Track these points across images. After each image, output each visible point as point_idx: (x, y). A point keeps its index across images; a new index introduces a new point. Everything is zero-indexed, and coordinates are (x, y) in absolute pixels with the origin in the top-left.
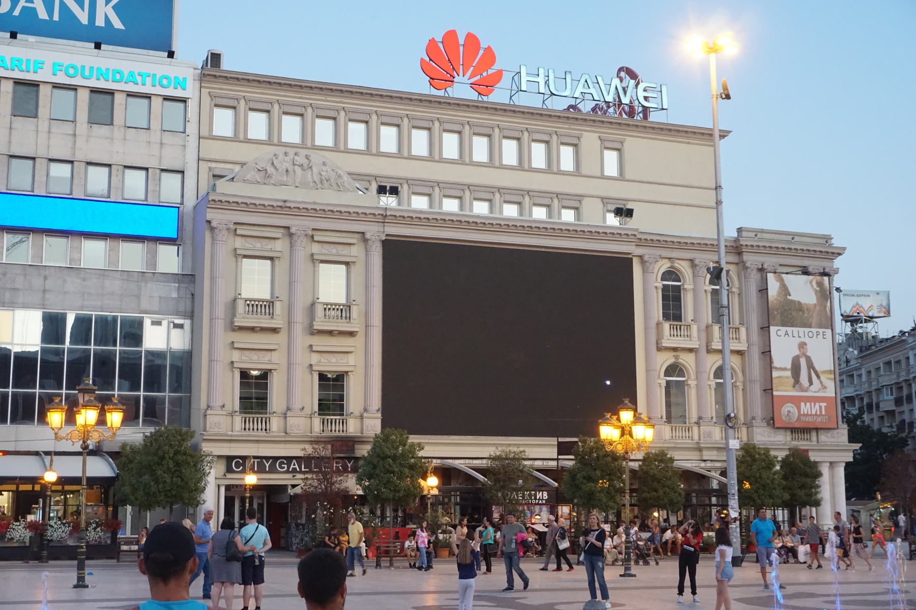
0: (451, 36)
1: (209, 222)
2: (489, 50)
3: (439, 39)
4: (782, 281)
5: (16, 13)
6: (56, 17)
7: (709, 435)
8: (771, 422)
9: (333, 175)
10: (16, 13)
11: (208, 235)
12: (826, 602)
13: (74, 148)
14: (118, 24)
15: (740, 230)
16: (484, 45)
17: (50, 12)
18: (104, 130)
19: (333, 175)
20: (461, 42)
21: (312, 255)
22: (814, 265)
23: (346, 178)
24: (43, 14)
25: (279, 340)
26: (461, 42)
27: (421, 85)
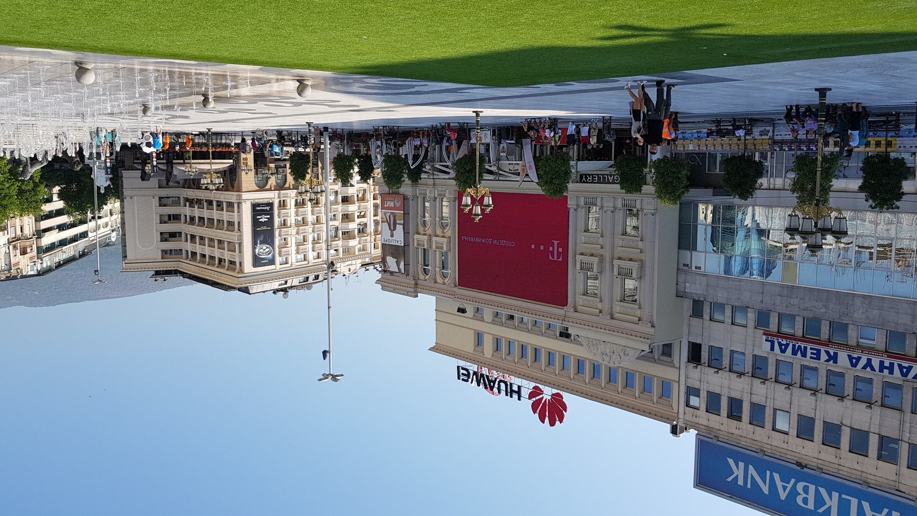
0: (552, 424)
1: (653, 326)
2: (535, 412)
3: (558, 423)
4: (399, 269)
5: (793, 481)
6: (768, 473)
7: (430, 192)
8: (405, 198)
9: (592, 348)
10: (793, 481)
11: (655, 320)
12: (187, 117)
13: (752, 385)
14: (731, 462)
15: (416, 296)
16: (537, 415)
17: (771, 476)
18: (734, 395)
19: (592, 348)
20: (547, 419)
21: (601, 301)
22: (388, 275)
23: (585, 344)
24: (776, 476)
25: (616, 255)
26: (547, 419)
27: (567, 398)
